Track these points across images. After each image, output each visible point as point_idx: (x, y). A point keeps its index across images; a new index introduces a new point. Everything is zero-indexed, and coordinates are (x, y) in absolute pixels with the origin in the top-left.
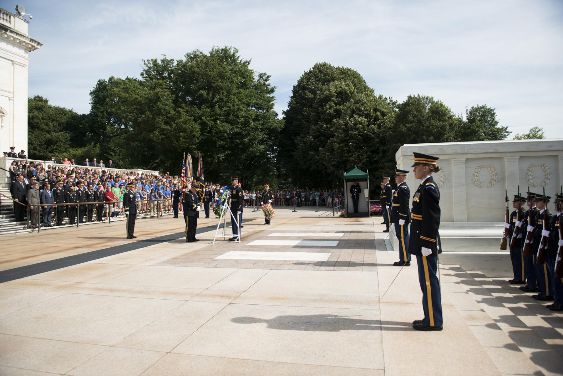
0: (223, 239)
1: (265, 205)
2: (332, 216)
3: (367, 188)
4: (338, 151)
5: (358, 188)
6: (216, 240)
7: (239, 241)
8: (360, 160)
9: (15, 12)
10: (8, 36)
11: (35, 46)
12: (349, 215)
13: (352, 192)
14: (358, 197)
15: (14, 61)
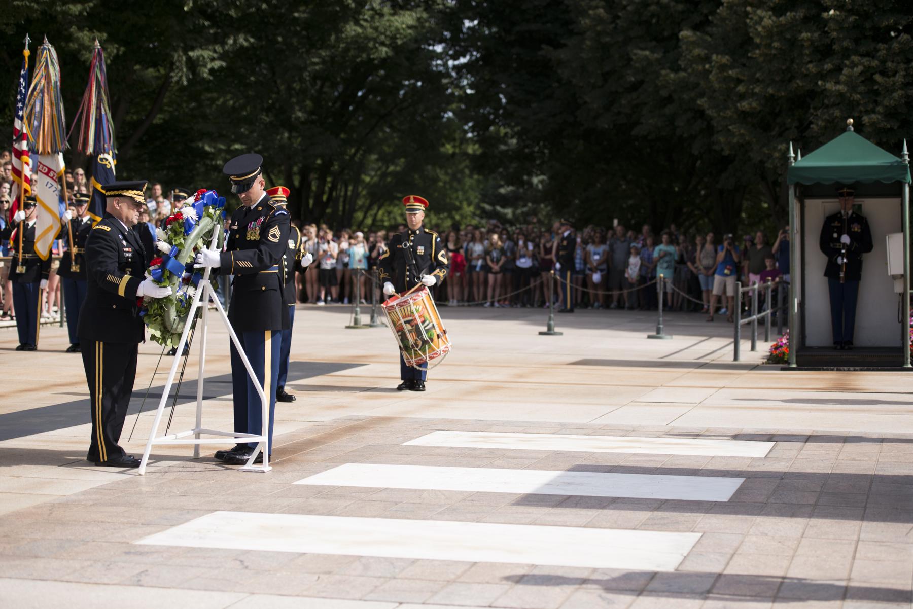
0: (191, 453)
1: (401, 299)
2: (729, 358)
3: (903, 230)
4: (769, 46)
5: (856, 228)
6: (155, 458)
7: (266, 467)
8: (874, 95)
14: (855, 271)
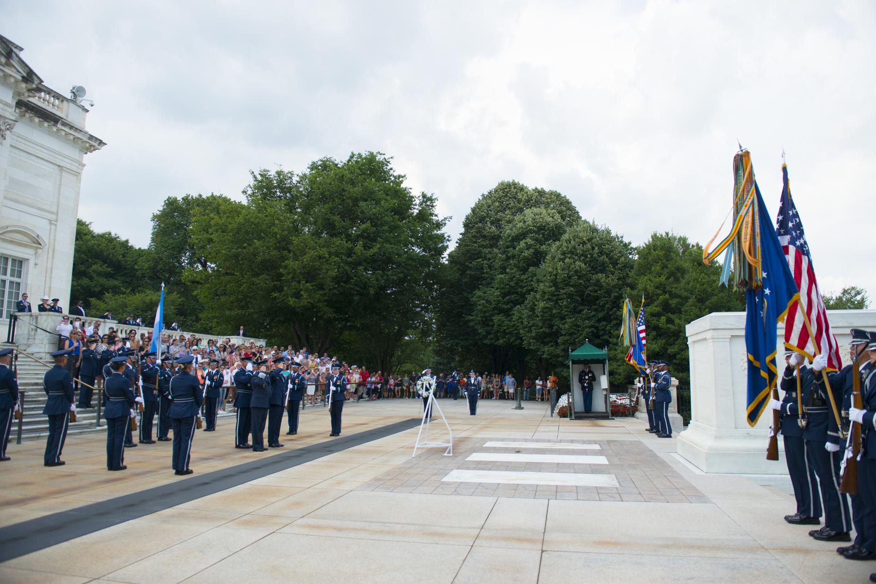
9: (69, 96)
10: (57, 130)
11: (94, 146)
12: (579, 417)
13: (581, 380)
15: (62, 167)
